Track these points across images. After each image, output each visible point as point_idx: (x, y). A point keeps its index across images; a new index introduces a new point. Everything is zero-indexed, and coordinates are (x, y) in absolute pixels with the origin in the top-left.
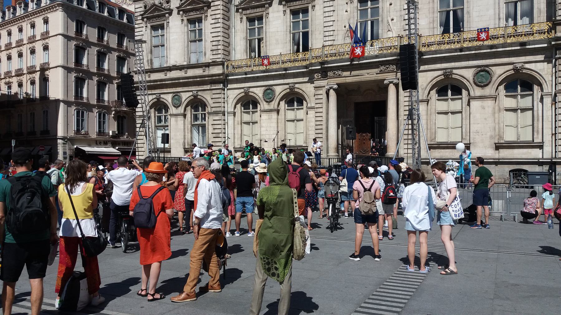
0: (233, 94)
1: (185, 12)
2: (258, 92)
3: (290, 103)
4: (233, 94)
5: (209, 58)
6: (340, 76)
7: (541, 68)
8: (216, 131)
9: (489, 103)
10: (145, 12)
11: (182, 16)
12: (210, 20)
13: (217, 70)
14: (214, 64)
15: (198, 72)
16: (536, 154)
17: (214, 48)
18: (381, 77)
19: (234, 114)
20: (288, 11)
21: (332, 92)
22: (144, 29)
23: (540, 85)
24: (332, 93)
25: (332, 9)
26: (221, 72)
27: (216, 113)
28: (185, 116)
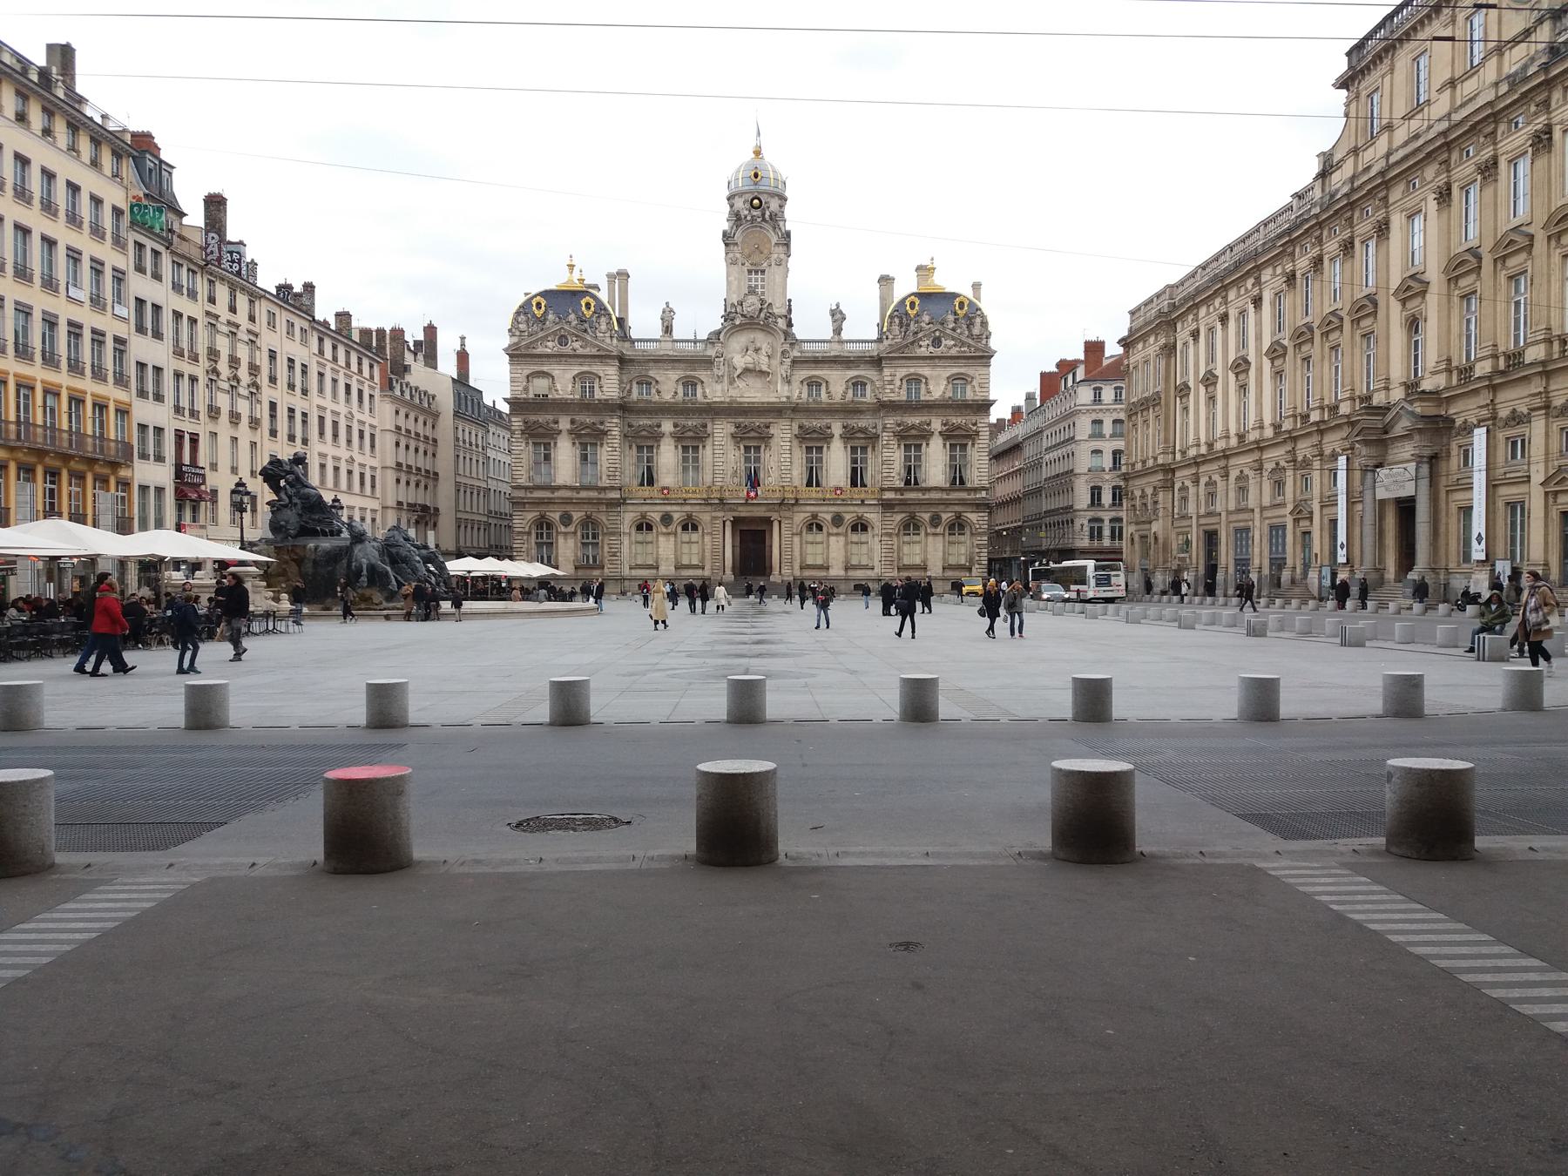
0: (629, 517)
1: (579, 436)
2: (656, 517)
3: (685, 528)
4: (629, 517)
5: (605, 482)
7: (873, 516)
9: (842, 539)
13: (615, 495)
14: (612, 488)
16: (870, 573)
27: (613, 534)
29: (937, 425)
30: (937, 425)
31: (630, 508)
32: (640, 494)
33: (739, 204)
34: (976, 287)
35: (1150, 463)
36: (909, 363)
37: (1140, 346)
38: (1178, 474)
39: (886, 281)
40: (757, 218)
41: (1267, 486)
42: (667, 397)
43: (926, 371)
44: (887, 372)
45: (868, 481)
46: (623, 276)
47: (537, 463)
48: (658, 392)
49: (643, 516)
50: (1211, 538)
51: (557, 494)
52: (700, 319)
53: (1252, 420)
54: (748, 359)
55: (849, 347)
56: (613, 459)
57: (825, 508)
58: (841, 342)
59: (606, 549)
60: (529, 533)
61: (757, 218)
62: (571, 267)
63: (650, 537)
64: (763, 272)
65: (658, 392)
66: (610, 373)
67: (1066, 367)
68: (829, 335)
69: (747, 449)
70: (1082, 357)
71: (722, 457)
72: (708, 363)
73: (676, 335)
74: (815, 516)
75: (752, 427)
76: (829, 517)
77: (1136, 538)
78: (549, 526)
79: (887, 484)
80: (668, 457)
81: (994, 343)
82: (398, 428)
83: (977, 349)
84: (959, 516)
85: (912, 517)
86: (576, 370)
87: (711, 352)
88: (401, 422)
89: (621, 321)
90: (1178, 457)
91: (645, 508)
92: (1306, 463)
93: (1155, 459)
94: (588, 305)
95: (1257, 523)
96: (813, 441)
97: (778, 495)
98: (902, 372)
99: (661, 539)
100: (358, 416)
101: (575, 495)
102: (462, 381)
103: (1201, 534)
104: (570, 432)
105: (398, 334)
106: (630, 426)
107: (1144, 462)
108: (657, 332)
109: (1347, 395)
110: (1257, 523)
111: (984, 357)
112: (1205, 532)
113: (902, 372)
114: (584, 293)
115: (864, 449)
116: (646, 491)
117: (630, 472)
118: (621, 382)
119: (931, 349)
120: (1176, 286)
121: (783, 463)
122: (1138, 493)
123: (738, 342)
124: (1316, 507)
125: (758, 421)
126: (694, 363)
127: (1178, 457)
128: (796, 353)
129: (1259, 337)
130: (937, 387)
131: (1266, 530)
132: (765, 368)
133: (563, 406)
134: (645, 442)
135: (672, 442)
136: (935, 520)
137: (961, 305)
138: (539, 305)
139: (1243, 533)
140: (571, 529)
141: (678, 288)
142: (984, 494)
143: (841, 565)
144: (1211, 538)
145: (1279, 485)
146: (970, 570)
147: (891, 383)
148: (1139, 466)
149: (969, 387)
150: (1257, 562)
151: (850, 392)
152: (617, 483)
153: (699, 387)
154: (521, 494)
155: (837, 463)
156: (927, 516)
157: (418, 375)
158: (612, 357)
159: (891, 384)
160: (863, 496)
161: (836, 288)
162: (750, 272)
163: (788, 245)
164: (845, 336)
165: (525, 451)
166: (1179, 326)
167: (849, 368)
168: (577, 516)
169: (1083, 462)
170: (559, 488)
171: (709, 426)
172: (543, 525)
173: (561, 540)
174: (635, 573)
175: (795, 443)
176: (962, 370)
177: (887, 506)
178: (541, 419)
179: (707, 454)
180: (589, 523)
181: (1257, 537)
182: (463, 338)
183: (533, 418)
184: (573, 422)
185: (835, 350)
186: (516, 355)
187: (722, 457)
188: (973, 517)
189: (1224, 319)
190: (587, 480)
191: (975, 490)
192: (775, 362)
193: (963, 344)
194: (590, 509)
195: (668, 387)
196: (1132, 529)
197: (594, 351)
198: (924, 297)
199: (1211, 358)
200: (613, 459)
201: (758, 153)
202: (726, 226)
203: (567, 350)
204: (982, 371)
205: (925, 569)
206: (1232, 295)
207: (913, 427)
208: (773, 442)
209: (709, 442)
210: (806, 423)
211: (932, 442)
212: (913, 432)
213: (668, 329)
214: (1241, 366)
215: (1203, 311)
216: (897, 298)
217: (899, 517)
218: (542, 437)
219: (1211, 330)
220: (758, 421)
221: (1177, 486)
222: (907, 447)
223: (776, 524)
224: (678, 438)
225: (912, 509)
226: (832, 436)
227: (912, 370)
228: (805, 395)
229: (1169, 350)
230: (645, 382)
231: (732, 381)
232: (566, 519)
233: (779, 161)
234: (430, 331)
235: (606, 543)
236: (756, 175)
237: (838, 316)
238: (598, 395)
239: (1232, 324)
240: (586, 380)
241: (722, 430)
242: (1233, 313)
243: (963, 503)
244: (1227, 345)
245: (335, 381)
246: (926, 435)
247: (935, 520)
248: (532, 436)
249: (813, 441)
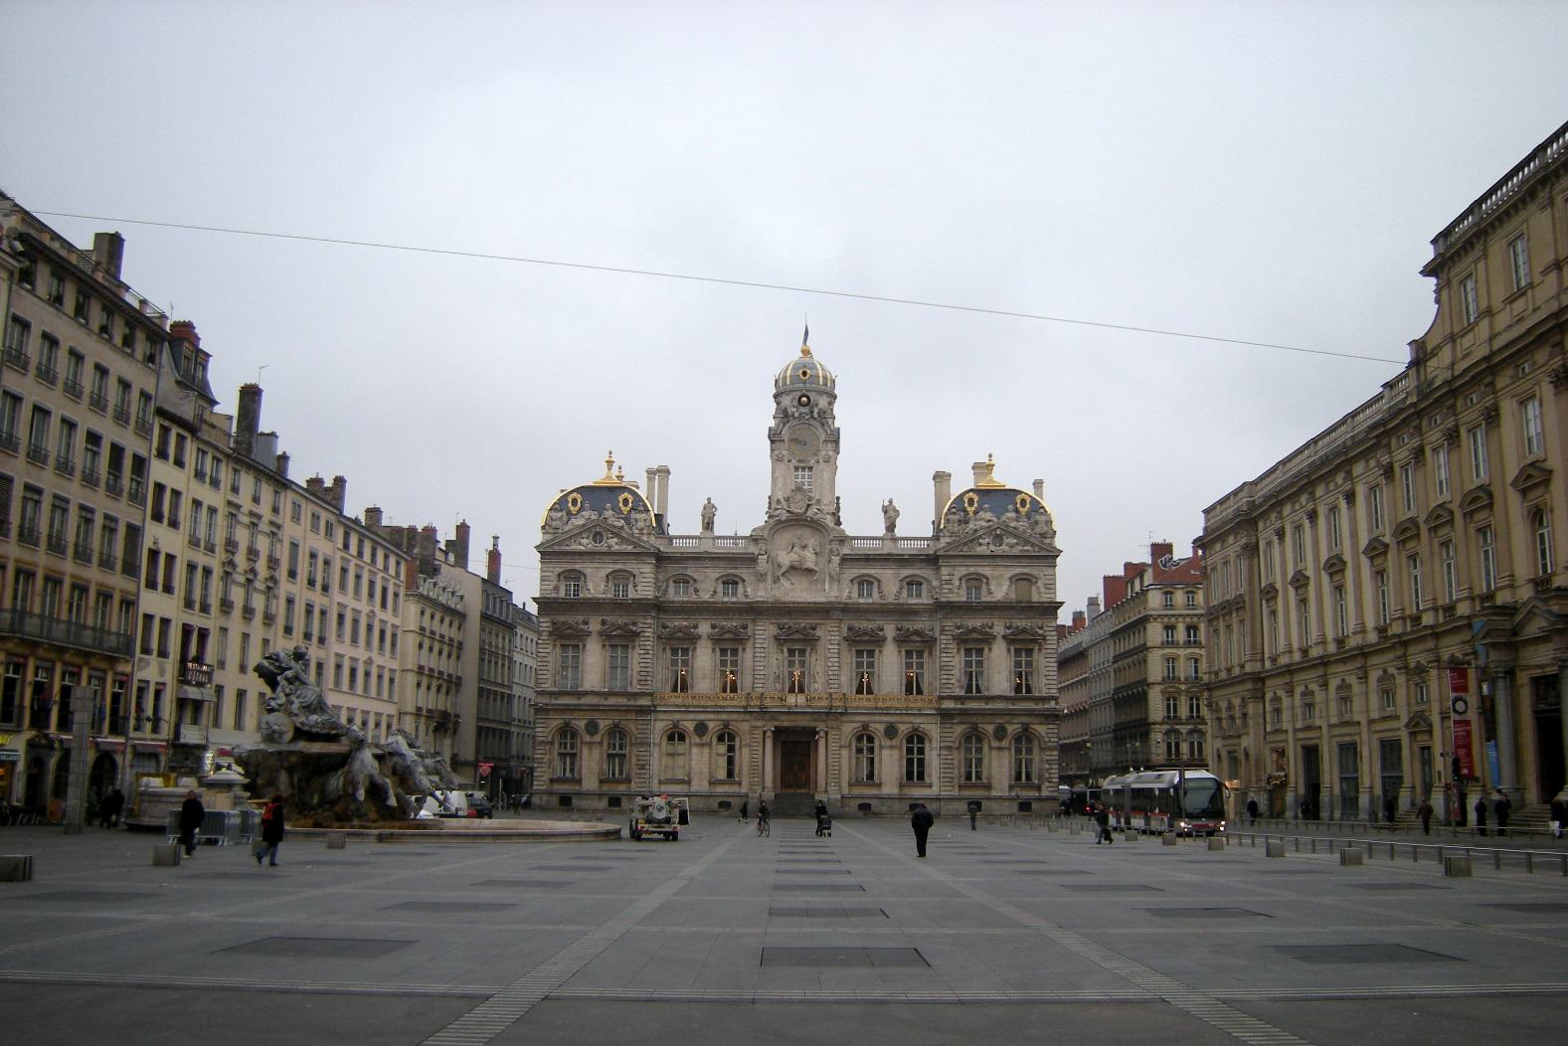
0: (659, 726)
1: (610, 637)
2: (690, 726)
4: (659, 726)
5: (636, 688)
6: (776, 720)
8: (641, 762)
10: (556, 629)
11: (603, 641)
12: (638, 650)
13: (645, 702)
15: (623, 701)
17: (642, 678)
18: (812, 724)
19: (660, 744)
20: (717, 649)
21: (769, 734)
22: (550, 647)
23: (930, 741)
24: (769, 734)
25: (763, 655)
26: (650, 703)
27: (642, 744)
28: (601, 743)
29: (999, 628)
30: (999, 628)
31: (661, 716)
32: (673, 700)
33: (786, 401)
34: (1038, 484)
35: (1236, 671)
36: (968, 562)
37: (1218, 546)
38: (1269, 683)
39: (941, 478)
40: (804, 413)
41: (1374, 700)
42: (706, 596)
43: (986, 571)
44: (944, 571)
45: (925, 688)
46: (664, 472)
47: (564, 668)
48: (696, 591)
49: (676, 725)
50: (1311, 754)
51: (584, 701)
52: (743, 515)
53: (1352, 624)
54: (794, 556)
55: (902, 544)
56: (646, 664)
57: (877, 718)
58: (895, 539)
59: (634, 759)
60: (552, 743)
61: (804, 413)
62: (610, 463)
63: (681, 748)
64: (810, 469)
65: (696, 591)
66: (646, 571)
67: (1134, 570)
68: (881, 531)
69: (791, 652)
70: (1149, 561)
71: (763, 661)
72: (751, 560)
73: (717, 532)
74: (865, 727)
75: (797, 629)
76: (881, 728)
77: (1224, 754)
78: (574, 734)
79: (947, 692)
80: (704, 658)
81: (1058, 543)
82: (422, 629)
83: (1041, 548)
84: (1026, 728)
85: (975, 727)
86: (610, 568)
87: (753, 549)
88: (426, 622)
89: (659, 517)
90: (1268, 665)
91: (677, 717)
92: (1421, 670)
93: (1242, 666)
94: (626, 501)
95: (1365, 736)
96: (864, 645)
97: (824, 703)
98: (962, 571)
99: (695, 750)
100: (380, 615)
101: (602, 701)
102: (491, 583)
103: (1300, 751)
104: (600, 634)
105: (430, 532)
106: (664, 627)
107: (1229, 670)
108: (697, 529)
109: (1465, 594)
110: (1365, 736)
111: (1050, 557)
112: (1304, 747)
113: (962, 571)
114: (624, 489)
115: (920, 654)
116: (678, 699)
117: (661, 681)
118: (657, 579)
119: (992, 548)
120: (1255, 483)
121: (830, 669)
122: (1223, 705)
123: (787, 537)
124: (1436, 719)
125: (803, 623)
126: (735, 562)
127: (1268, 665)
128: (846, 550)
129: (1354, 535)
130: (1000, 589)
131: (1376, 745)
132: (811, 565)
133: (595, 606)
134: (680, 644)
135: (710, 644)
136: (1000, 734)
137: (1023, 502)
138: (574, 502)
139: (1349, 751)
140: (597, 738)
141: (719, 482)
142: (1053, 704)
143: (896, 782)
144: (1311, 754)
145: (1387, 694)
146: (1039, 788)
147: (949, 582)
148: (1223, 675)
149: (1034, 588)
150: (1366, 782)
151: (905, 591)
152: (647, 689)
153: (740, 586)
154: (545, 700)
155: (890, 666)
156: (990, 728)
157: (448, 573)
158: (647, 554)
159: (951, 584)
160: (919, 704)
161: (888, 481)
162: (797, 468)
163: (837, 442)
164: (899, 532)
165: (552, 654)
166: (1261, 525)
167: (904, 567)
168: (604, 724)
169: (1155, 670)
170: (586, 693)
171: (750, 627)
172: (567, 732)
173: (585, 751)
174: (663, 788)
175: (845, 645)
176: (1026, 570)
177: (945, 716)
178: (570, 619)
179: (747, 657)
180: (617, 732)
181: (1365, 753)
182: (496, 538)
183: (562, 619)
184: (603, 623)
185: (888, 548)
186: (547, 553)
187: (763, 661)
188: (1041, 729)
189: (1313, 516)
190: (618, 686)
191: (1044, 699)
192: (823, 560)
193: (1027, 542)
194: (616, 717)
195: (707, 586)
196: (1218, 743)
197: (630, 548)
198: (985, 494)
199: (1300, 556)
200: (646, 664)
201: (806, 352)
202: (772, 423)
203: (602, 547)
204: (1049, 571)
205: (989, 787)
206: (1320, 491)
207: (974, 630)
208: (822, 642)
209: (749, 644)
210: (856, 624)
211: (995, 647)
212: (975, 635)
213: (708, 525)
214: (1335, 566)
215: (1287, 509)
216: (955, 490)
217: (959, 729)
218: (569, 639)
219: (1298, 528)
220: (803, 623)
221: (1269, 696)
222: (968, 652)
223: (822, 734)
224: (716, 640)
225: (974, 719)
226: (884, 639)
227: (972, 569)
228: (855, 595)
229: (1252, 550)
230: (684, 580)
231: (776, 580)
232: (592, 728)
233: (828, 359)
234: (463, 530)
235: (633, 754)
236: (805, 374)
237: (890, 514)
238: (632, 595)
239: (1322, 522)
240: (619, 578)
241: (764, 632)
242: (1322, 510)
243: (1030, 713)
244: (1316, 545)
245: (358, 577)
246: (988, 639)
247: (1000, 734)
248: (560, 637)
249: (864, 645)
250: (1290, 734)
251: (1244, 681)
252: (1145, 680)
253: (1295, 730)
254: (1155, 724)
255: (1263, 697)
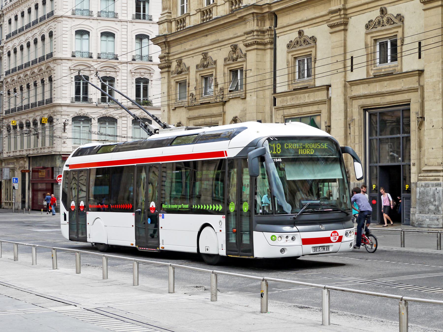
35: (194, 20)
38: (282, 21)
103: (356, 113)
122: (192, 62)
250: (337, 94)
251: (242, 20)
252: (50, 55)
253: (349, 84)
254: (60, 105)
255: (274, 43)
